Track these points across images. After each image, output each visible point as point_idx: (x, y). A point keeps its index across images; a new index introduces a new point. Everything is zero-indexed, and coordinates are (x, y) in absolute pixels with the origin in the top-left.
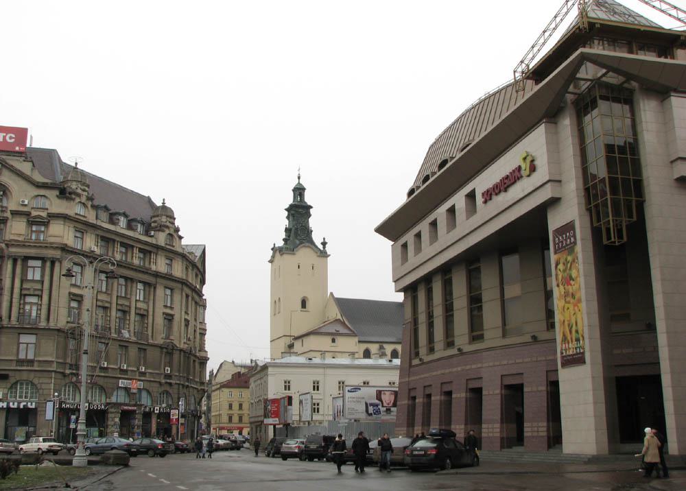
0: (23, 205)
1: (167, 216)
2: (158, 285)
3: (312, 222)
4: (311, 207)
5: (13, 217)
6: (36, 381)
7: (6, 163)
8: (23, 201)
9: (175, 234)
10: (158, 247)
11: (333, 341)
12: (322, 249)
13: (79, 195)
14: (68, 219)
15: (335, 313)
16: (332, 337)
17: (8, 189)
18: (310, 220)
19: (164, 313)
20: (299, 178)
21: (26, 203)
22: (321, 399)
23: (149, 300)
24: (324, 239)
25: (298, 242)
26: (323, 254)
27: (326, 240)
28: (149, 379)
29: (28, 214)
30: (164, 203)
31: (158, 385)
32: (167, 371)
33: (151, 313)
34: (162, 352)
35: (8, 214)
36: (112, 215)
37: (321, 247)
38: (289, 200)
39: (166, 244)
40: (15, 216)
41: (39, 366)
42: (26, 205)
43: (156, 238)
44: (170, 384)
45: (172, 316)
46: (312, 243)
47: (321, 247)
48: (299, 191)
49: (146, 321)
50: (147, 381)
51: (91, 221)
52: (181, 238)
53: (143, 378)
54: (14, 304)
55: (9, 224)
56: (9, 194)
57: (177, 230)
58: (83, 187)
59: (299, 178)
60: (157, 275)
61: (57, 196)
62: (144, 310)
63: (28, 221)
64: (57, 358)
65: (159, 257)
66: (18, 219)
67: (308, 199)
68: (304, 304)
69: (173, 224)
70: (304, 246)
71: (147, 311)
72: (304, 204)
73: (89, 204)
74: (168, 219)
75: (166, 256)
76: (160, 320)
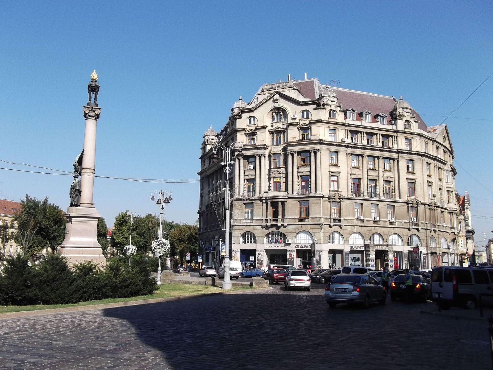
6: (311, 231)
8: (294, 116)
10: (397, 132)
29: (296, 124)
32: (414, 220)
34: (408, 207)
41: (312, 222)
64: (324, 214)
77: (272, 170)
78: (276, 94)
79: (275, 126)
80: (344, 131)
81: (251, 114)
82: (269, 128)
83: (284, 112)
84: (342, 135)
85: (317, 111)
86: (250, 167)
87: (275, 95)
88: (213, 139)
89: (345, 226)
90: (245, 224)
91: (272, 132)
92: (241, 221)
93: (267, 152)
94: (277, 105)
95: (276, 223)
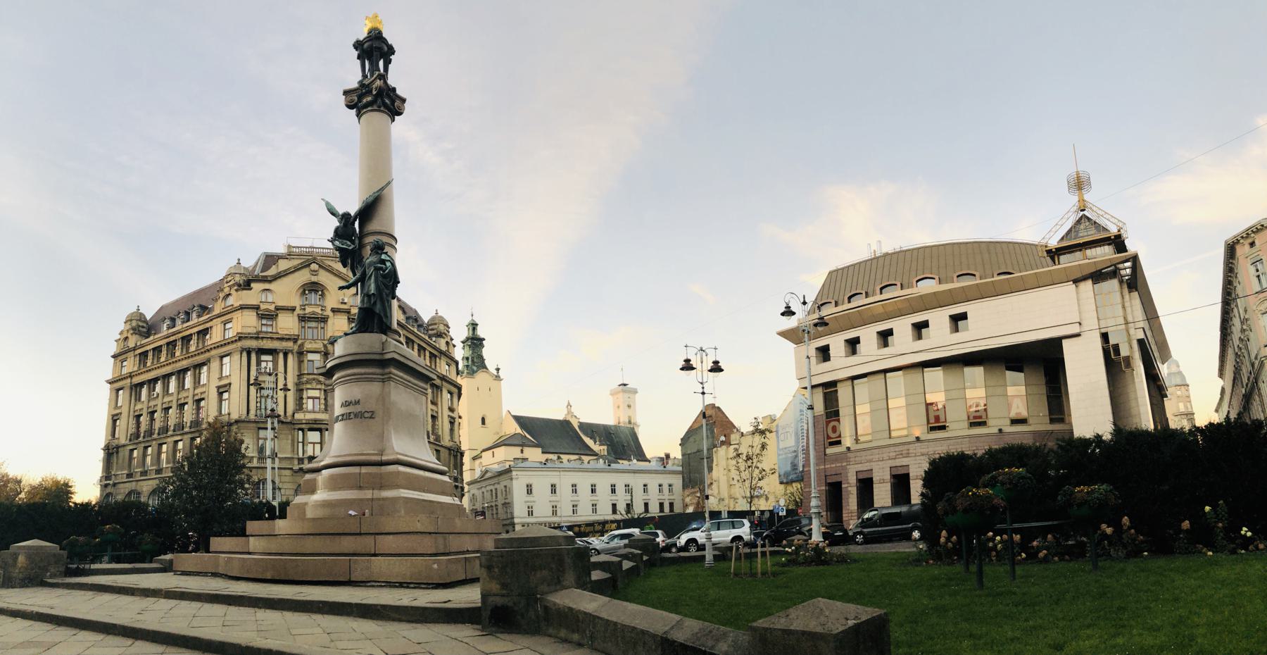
0: (342, 303)
3: (486, 352)
4: (484, 339)
8: (343, 300)
10: (441, 352)
11: (522, 451)
16: (521, 448)
21: (346, 301)
25: (475, 368)
27: (499, 367)
35: (328, 312)
42: (345, 303)
55: (330, 322)
60: (443, 378)
63: (349, 319)
66: (339, 317)
67: (481, 332)
69: (449, 332)
78: (314, 262)
79: (309, 310)
81: (267, 286)
82: (298, 311)
83: (325, 291)
86: (266, 368)
87: (311, 264)
91: (302, 319)
93: (296, 348)
94: (314, 279)
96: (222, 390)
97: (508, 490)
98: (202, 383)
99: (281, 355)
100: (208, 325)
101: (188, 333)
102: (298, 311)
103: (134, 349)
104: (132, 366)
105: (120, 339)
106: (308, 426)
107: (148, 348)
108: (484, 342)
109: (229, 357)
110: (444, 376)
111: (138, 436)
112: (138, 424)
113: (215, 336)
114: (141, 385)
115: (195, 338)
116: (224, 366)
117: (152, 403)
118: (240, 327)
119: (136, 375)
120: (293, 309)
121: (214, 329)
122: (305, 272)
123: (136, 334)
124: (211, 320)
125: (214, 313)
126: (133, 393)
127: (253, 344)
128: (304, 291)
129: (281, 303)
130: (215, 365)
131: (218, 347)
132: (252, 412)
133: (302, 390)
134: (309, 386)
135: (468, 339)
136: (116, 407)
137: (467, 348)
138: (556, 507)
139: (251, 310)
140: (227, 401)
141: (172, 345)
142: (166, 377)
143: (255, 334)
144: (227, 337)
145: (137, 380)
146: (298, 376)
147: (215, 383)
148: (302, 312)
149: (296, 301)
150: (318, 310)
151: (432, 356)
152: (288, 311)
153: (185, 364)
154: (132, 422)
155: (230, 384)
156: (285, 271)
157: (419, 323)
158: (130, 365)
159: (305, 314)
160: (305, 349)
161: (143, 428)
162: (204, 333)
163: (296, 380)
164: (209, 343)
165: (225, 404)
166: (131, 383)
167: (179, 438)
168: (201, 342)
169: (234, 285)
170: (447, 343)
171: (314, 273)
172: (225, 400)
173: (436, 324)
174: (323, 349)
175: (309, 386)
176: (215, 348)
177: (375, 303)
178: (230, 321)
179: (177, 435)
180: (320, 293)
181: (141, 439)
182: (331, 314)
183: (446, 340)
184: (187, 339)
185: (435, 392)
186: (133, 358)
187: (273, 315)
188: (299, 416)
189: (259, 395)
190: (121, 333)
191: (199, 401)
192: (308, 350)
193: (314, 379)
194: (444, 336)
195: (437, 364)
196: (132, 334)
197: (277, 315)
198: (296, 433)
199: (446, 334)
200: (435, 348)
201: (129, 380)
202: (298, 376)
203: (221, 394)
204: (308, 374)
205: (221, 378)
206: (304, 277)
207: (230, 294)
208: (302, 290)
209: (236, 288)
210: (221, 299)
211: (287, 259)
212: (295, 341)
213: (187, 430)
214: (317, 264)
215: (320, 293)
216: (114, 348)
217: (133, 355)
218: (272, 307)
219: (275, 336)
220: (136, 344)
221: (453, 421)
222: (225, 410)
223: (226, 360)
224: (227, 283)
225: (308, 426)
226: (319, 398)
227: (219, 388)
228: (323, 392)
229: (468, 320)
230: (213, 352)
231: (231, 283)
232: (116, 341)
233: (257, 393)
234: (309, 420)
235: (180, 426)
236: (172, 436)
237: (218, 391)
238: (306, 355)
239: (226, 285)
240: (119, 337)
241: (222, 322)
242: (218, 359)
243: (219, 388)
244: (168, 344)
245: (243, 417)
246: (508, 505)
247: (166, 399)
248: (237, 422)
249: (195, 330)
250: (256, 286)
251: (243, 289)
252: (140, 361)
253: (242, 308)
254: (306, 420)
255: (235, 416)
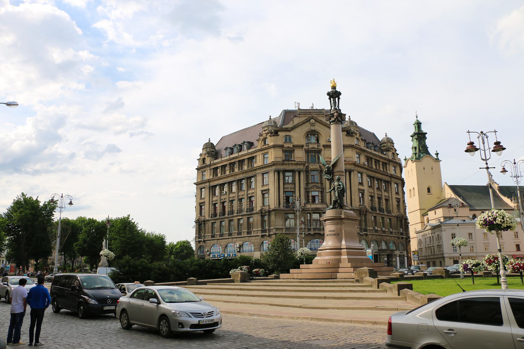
1: (391, 143)
2: (392, 182)
3: (428, 142)
4: (426, 133)
5: (324, 149)
7: (318, 119)
9: (395, 154)
10: (389, 161)
12: (436, 157)
13: (356, 134)
14: (354, 147)
15: (449, 194)
17: (319, 133)
18: (426, 141)
19: (396, 198)
20: (417, 117)
22: (474, 244)
23: (388, 190)
24: (437, 151)
26: (437, 160)
28: (394, 236)
30: (386, 136)
31: (396, 239)
33: (390, 198)
34: (397, 220)
36: (368, 144)
37: (435, 156)
38: (413, 130)
39: (392, 159)
40: (325, 148)
43: (388, 156)
44: (402, 238)
45: (399, 199)
46: (429, 154)
47: (435, 156)
48: (418, 124)
49: (389, 203)
50: (394, 236)
51: (362, 148)
52: (398, 154)
53: (392, 235)
54: (332, 197)
55: (322, 153)
56: (320, 136)
57: (396, 151)
58: (357, 129)
59: (417, 117)
60: (391, 176)
61: (346, 135)
62: (388, 196)
65: (390, 166)
67: (424, 129)
68: (429, 190)
69: (394, 146)
70: (426, 156)
71: (389, 197)
72: (421, 132)
73: (360, 138)
74: (392, 144)
75: (393, 165)
76: (395, 203)
77: (310, 186)
78: (312, 118)
79: (311, 146)
80: (364, 156)
81: (288, 133)
82: (305, 147)
83: (319, 135)
84: (363, 160)
85: (348, 137)
86: (288, 180)
87: (311, 119)
88: (213, 152)
89: (370, 234)
90: (288, 232)
91: (307, 152)
92: (284, 230)
94: (313, 128)
95: (320, 232)
96: (264, 192)
97: (440, 237)
98: (252, 188)
99: (297, 173)
100: (254, 155)
101: (242, 158)
102: (305, 147)
103: (210, 165)
104: (209, 175)
105: (200, 159)
106: (312, 212)
107: (218, 165)
108: (426, 135)
109: (267, 174)
110: (392, 175)
111: (215, 215)
112: (215, 208)
113: (259, 162)
114: (215, 186)
115: (246, 162)
116: (265, 179)
117: (223, 197)
118: (273, 158)
119: (212, 181)
120: (302, 146)
121: (258, 157)
122: (308, 124)
123: (210, 156)
124: (256, 152)
125: (257, 149)
126: (211, 191)
127: (281, 167)
128: (308, 135)
129: (296, 143)
130: (259, 178)
131: (261, 168)
132: (282, 205)
133: (309, 192)
134: (312, 190)
135: (415, 134)
136: (201, 198)
137: (415, 140)
138: (473, 247)
139: (278, 148)
140: (267, 199)
141: (232, 165)
142: (230, 183)
143: (282, 162)
144: (265, 163)
145: (212, 184)
146: (306, 184)
147: (259, 189)
148: (307, 148)
149: (303, 142)
150: (316, 146)
151: (384, 164)
152: (299, 148)
153: (241, 176)
154: (212, 207)
155: (269, 189)
156: (297, 124)
157: (374, 145)
158: (208, 175)
159: (309, 149)
160: (310, 169)
161: (219, 210)
162: (251, 159)
163: (305, 187)
164: (255, 165)
165: (266, 200)
166: (209, 185)
167: (240, 217)
168: (250, 164)
169: (268, 133)
170: (393, 153)
171: (313, 125)
172: (266, 198)
173: (385, 143)
174: (319, 169)
175: (312, 190)
176: (259, 168)
177: (338, 199)
178: (267, 153)
179: (239, 216)
180: (316, 136)
181: (218, 217)
182: (323, 148)
183: (392, 152)
184: (241, 162)
185: (387, 185)
186: (209, 171)
187: (292, 150)
188: (308, 206)
189: (285, 195)
190: (201, 155)
191: (250, 197)
192: (312, 169)
193: (315, 185)
194: (390, 150)
195: (388, 168)
196: (208, 157)
197: (294, 150)
198: (306, 215)
199: (392, 149)
200: (385, 159)
201: (208, 184)
202: (306, 184)
203: (263, 195)
204: (312, 183)
205: (263, 185)
206: (306, 128)
207: (266, 138)
208: (306, 135)
209: (270, 134)
210: (261, 141)
211: (298, 117)
212: (304, 165)
213: (245, 213)
214: (314, 119)
215: (316, 136)
216: (196, 164)
217: (209, 169)
218: (291, 146)
219: (294, 162)
220: (211, 162)
221: (398, 200)
222: (266, 203)
223: (265, 176)
224: (264, 131)
225: (312, 212)
226: (318, 196)
227: (262, 191)
228: (320, 193)
229: (414, 120)
230: (258, 171)
231: (266, 132)
232: (198, 160)
233: (284, 194)
234: (313, 208)
235: (240, 211)
236: (237, 216)
237: (262, 193)
238: (310, 172)
239: (264, 132)
240: (199, 157)
241: (262, 154)
242: (261, 175)
243: (262, 191)
244: (230, 164)
245: (277, 208)
246: (440, 246)
247: (231, 195)
248: (273, 210)
249: (247, 157)
250: (281, 134)
251: (274, 136)
252: (213, 172)
253: (274, 146)
254: (312, 208)
255: (272, 207)
